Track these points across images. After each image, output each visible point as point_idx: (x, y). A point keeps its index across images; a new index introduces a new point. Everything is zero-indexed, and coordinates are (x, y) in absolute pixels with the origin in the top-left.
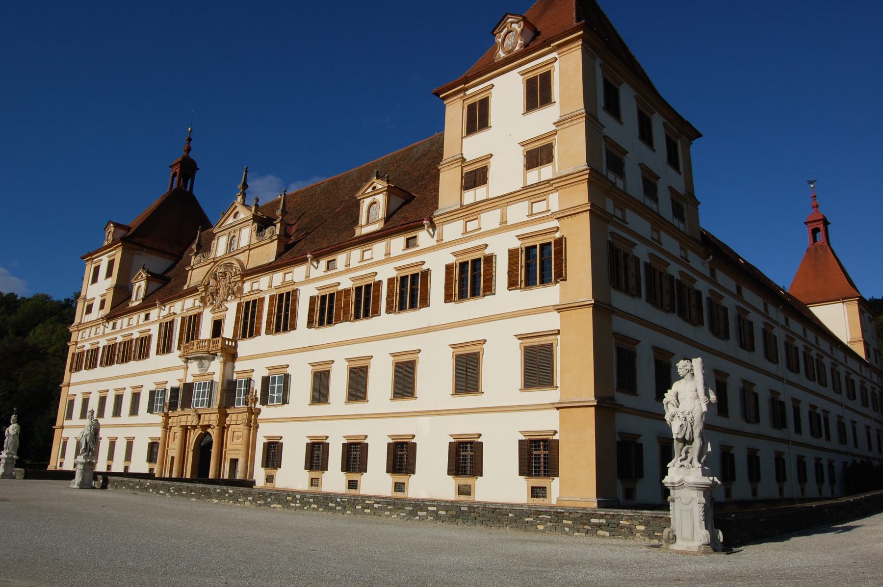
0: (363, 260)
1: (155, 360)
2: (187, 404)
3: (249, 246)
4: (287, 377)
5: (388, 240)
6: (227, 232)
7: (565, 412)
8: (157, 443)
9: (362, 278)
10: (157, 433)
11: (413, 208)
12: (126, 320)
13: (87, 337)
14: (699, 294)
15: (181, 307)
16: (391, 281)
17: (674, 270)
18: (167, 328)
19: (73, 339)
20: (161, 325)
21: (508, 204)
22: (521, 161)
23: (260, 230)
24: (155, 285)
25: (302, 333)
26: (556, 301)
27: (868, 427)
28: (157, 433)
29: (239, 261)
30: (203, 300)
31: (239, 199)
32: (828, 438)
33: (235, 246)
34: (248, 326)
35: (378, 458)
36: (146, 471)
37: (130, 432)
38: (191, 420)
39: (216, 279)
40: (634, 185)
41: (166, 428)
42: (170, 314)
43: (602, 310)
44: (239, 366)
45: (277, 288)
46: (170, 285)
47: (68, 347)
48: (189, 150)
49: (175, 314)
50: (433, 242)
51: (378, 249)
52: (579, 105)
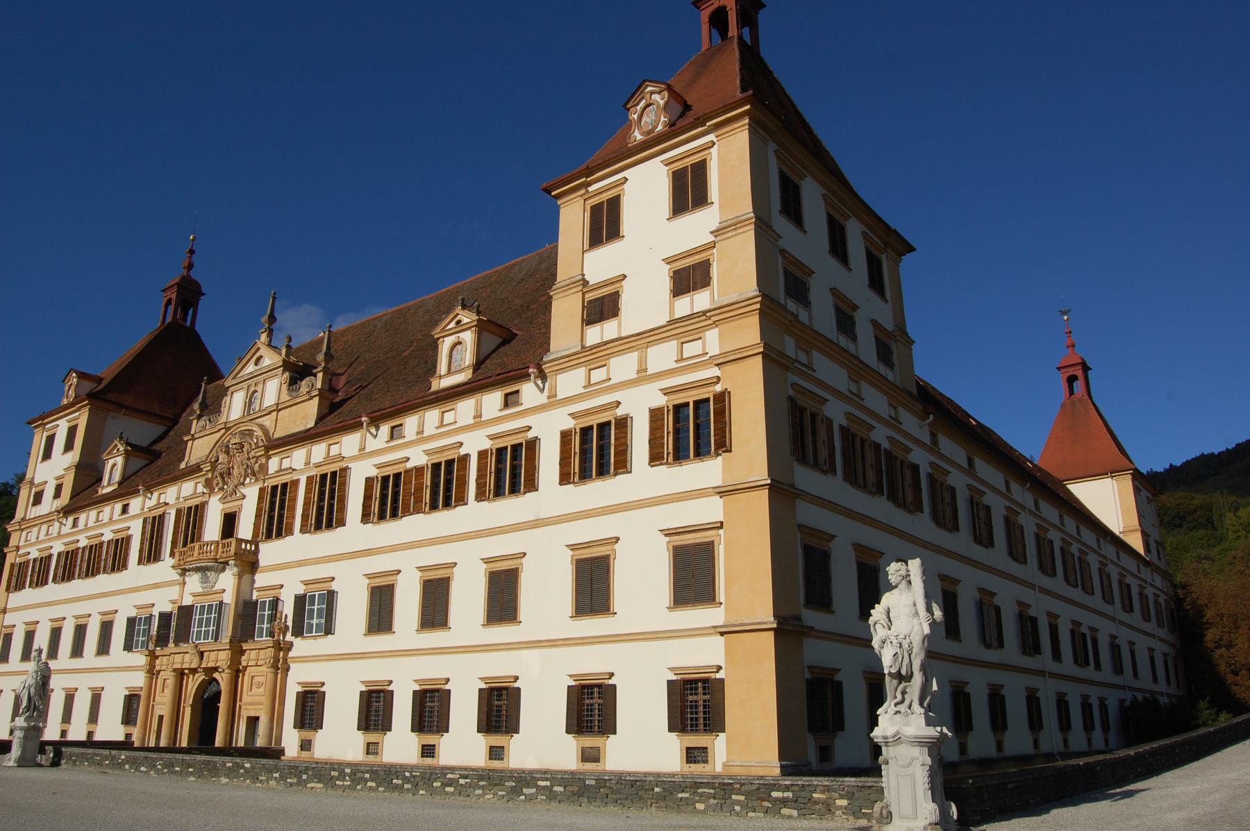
0: (442, 425)
1: (135, 572)
2: (183, 637)
3: (277, 405)
4: (331, 597)
5: (478, 396)
6: (245, 385)
7: (731, 637)
8: (138, 696)
9: (442, 450)
10: (138, 680)
11: (513, 352)
12: (93, 514)
13: (33, 540)
14: (915, 468)
15: (177, 495)
16: (482, 455)
17: (880, 435)
18: (155, 526)
19: (13, 542)
21: (649, 345)
22: (666, 284)
23: (293, 382)
24: (138, 462)
25: (354, 531)
26: (718, 482)
27: (1151, 650)
28: (138, 680)
29: (262, 427)
30: (208, 484)
31: (264, 337)
32: (1098, 666)
33: (256, 406)
34: (275, 522)
35: (464, 710)
36: (121, 738)
37: (96, 680)
38: (190, 661)
39: (227, 453)
40: (822, 317)
41: (152, 672)
42: (159, 505)
43: (782, 493)
44: (261, 579)
45: (318, 466)
46: (159, 462)
47: (5, 555)
48: (190, 267)
49: (166, 504)
50: (543, 399)
51: (464, 409)
52: (745, 206)
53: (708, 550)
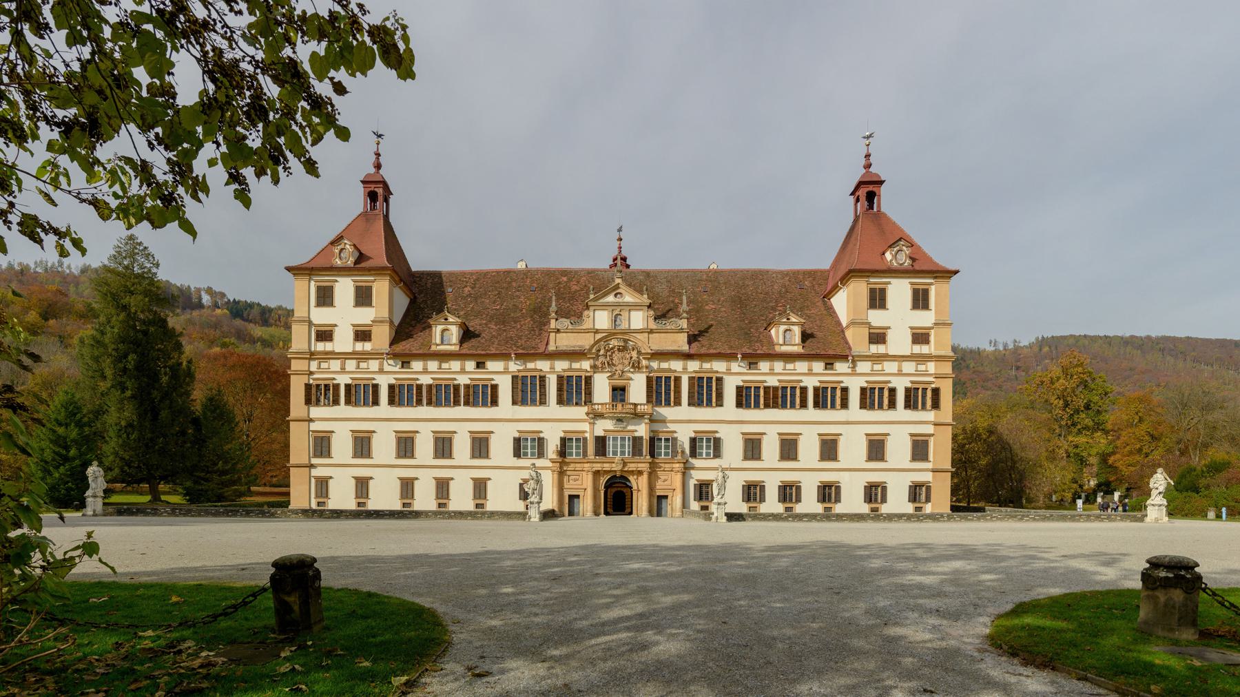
16: (816, 389)
19: (296, 365)
20: (514, 378)
50: (849, 371)
51: (802, 366)
53: (926, 443)
